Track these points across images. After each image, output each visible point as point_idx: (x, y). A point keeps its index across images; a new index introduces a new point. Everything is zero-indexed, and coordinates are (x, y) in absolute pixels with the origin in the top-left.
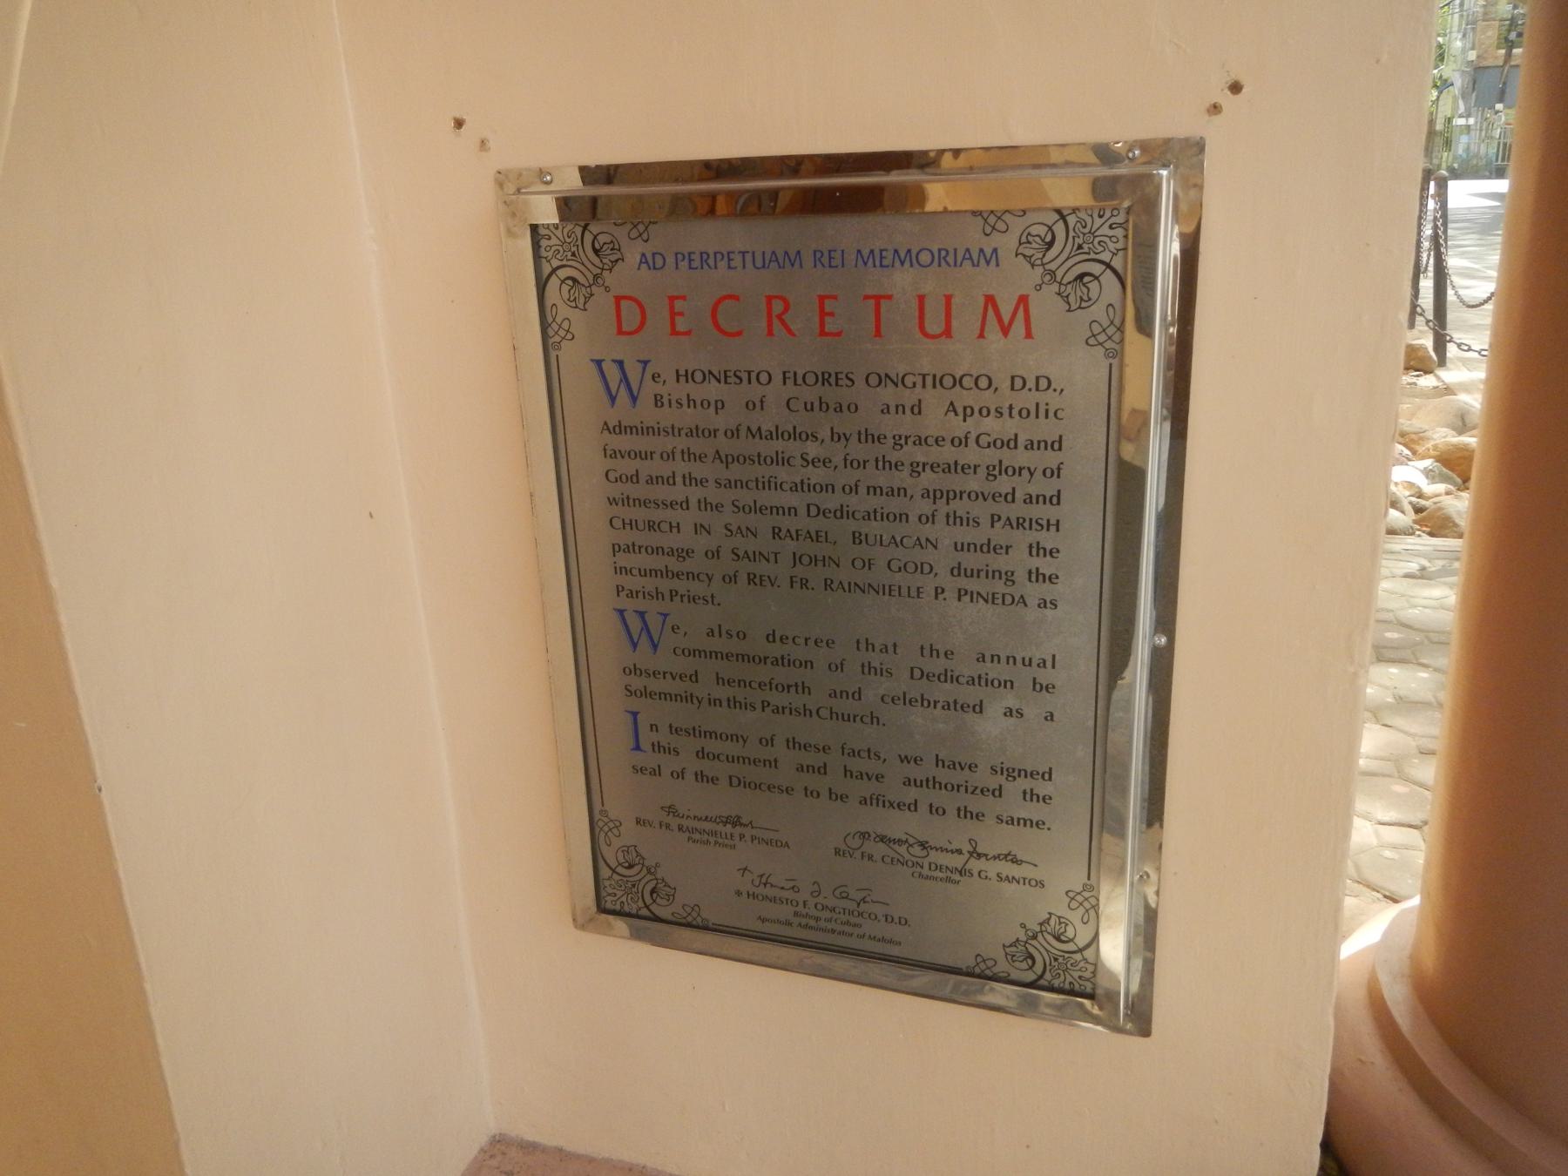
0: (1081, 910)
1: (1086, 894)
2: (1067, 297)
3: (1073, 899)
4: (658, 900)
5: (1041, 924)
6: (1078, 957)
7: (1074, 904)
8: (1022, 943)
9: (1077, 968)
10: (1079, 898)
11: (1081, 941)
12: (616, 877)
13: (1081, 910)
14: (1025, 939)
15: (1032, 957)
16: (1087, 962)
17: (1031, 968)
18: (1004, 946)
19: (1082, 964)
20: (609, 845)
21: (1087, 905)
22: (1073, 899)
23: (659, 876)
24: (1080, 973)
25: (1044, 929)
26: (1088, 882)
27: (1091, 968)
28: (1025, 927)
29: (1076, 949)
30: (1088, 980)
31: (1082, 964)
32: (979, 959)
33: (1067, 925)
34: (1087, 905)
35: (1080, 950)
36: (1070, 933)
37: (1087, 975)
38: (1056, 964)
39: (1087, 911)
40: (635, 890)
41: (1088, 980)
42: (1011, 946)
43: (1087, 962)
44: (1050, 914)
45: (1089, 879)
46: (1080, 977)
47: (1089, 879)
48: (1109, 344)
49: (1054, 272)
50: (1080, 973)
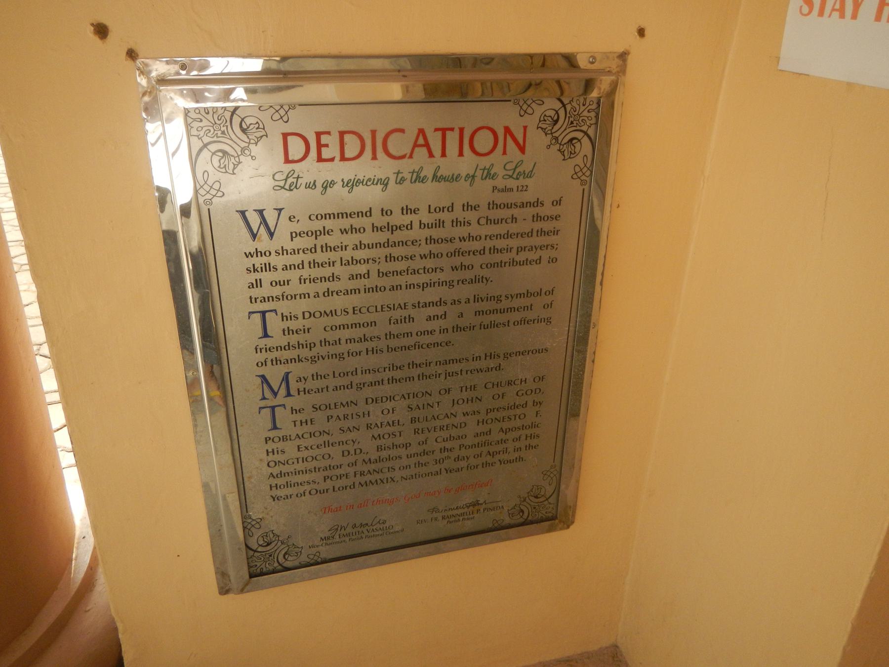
0: (210, 182)
1: (209, 196)
2: (274, 536)
3: (218, 190)
4: (552, 113)
5: (240, 163)
6: (206, 140)
7: (216, 186)
8: (254, 142)
9: (205, 129)
10: (213, 192)
11: (206, 154)
12: (585, 128)
13: (210, 182)
14: (251, 146)
15: (244, 131)
16: (198, 136)
17: (243, 120)
18: (267, 136)
19: (202, 133)
20: (586, 155)
21: (207, 187)
22: (218, 190)
23: (550, 136)
24: (201, 124)
25: (237, 159)
26: (208, 207)
27: (194, 132)
28: (252, 157)
29: (208, 147)
30: (194, 120)
31: (202, 133)
32: (285, 119)
33: (219, 167)
34: (207, 187)
35: (205, 146)
36: (216, 159)
37: (196, 124)
38: (223, 129)
39: (206, 183)
40: (571, 119)
41: (194, 120)
42: (261, 137)
43: (198, 136)
44: (234, 174)
45: (209, 209)
46: (201, 121)
47: (209, 209)
48: (249, 521)
49: (282, 544)
50: (201, 124)
